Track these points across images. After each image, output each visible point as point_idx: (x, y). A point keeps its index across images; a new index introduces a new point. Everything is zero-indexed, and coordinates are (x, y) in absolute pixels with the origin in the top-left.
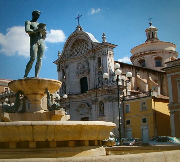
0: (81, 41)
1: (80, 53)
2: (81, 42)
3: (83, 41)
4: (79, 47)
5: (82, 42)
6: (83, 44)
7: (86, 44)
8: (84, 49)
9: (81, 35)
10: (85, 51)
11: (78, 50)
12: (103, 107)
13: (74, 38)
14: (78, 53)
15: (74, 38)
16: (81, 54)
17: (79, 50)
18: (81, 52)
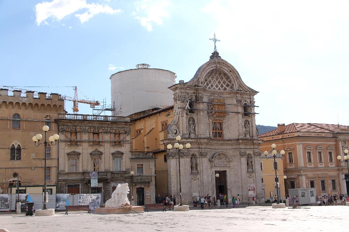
0: (218, 73)
1: (210, 85)
2: (217, 75)
3: (220, 74)
4: (210, 78)
5: (217, 75)
6: (217, 76)
7: (222, 78)
8: (217, 83)
9: (224, 67)
10: (217, 86)
11: (208, 82)
12: (251, 162)
13: (213, 66)
14: (208, 85)
15: (213, 66)
16: (211, 88)
17: (210, 82)
18: (212, 86)
